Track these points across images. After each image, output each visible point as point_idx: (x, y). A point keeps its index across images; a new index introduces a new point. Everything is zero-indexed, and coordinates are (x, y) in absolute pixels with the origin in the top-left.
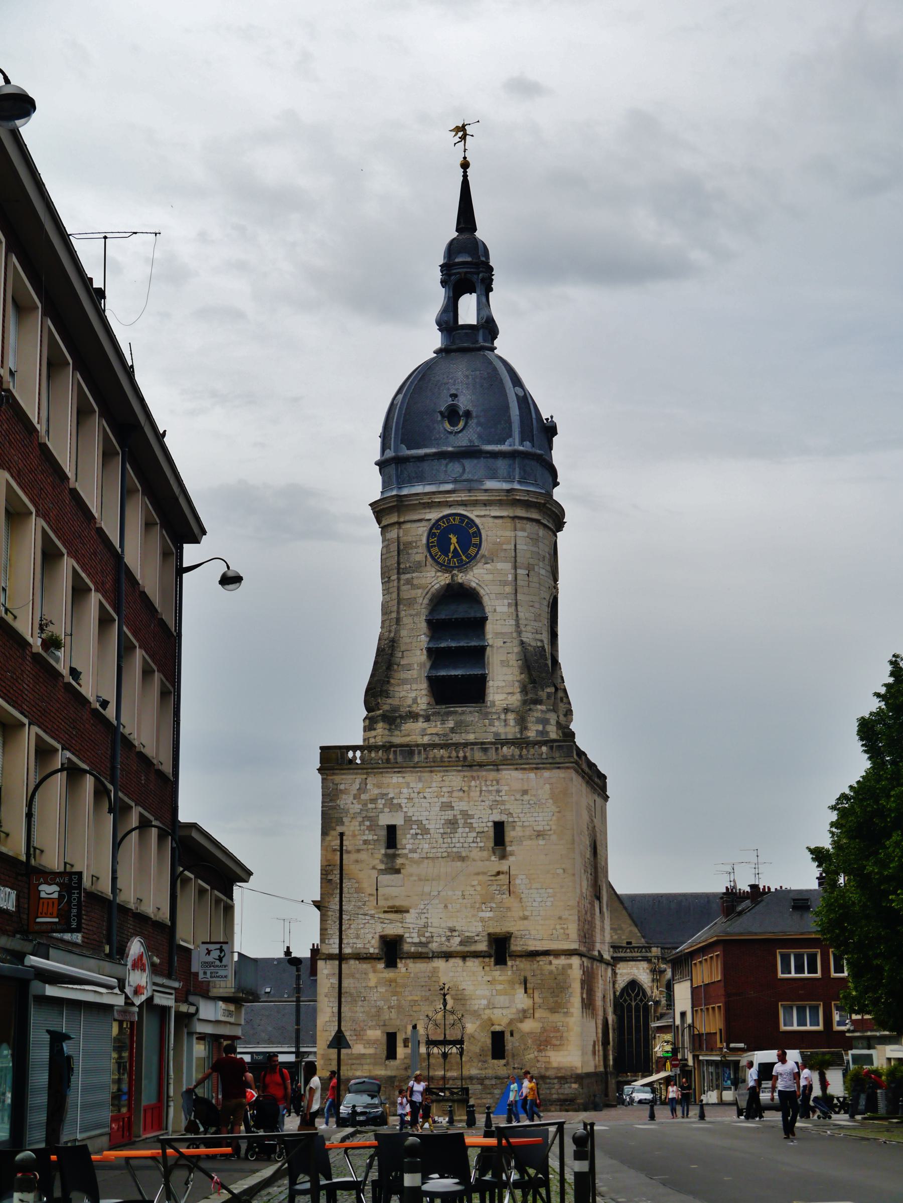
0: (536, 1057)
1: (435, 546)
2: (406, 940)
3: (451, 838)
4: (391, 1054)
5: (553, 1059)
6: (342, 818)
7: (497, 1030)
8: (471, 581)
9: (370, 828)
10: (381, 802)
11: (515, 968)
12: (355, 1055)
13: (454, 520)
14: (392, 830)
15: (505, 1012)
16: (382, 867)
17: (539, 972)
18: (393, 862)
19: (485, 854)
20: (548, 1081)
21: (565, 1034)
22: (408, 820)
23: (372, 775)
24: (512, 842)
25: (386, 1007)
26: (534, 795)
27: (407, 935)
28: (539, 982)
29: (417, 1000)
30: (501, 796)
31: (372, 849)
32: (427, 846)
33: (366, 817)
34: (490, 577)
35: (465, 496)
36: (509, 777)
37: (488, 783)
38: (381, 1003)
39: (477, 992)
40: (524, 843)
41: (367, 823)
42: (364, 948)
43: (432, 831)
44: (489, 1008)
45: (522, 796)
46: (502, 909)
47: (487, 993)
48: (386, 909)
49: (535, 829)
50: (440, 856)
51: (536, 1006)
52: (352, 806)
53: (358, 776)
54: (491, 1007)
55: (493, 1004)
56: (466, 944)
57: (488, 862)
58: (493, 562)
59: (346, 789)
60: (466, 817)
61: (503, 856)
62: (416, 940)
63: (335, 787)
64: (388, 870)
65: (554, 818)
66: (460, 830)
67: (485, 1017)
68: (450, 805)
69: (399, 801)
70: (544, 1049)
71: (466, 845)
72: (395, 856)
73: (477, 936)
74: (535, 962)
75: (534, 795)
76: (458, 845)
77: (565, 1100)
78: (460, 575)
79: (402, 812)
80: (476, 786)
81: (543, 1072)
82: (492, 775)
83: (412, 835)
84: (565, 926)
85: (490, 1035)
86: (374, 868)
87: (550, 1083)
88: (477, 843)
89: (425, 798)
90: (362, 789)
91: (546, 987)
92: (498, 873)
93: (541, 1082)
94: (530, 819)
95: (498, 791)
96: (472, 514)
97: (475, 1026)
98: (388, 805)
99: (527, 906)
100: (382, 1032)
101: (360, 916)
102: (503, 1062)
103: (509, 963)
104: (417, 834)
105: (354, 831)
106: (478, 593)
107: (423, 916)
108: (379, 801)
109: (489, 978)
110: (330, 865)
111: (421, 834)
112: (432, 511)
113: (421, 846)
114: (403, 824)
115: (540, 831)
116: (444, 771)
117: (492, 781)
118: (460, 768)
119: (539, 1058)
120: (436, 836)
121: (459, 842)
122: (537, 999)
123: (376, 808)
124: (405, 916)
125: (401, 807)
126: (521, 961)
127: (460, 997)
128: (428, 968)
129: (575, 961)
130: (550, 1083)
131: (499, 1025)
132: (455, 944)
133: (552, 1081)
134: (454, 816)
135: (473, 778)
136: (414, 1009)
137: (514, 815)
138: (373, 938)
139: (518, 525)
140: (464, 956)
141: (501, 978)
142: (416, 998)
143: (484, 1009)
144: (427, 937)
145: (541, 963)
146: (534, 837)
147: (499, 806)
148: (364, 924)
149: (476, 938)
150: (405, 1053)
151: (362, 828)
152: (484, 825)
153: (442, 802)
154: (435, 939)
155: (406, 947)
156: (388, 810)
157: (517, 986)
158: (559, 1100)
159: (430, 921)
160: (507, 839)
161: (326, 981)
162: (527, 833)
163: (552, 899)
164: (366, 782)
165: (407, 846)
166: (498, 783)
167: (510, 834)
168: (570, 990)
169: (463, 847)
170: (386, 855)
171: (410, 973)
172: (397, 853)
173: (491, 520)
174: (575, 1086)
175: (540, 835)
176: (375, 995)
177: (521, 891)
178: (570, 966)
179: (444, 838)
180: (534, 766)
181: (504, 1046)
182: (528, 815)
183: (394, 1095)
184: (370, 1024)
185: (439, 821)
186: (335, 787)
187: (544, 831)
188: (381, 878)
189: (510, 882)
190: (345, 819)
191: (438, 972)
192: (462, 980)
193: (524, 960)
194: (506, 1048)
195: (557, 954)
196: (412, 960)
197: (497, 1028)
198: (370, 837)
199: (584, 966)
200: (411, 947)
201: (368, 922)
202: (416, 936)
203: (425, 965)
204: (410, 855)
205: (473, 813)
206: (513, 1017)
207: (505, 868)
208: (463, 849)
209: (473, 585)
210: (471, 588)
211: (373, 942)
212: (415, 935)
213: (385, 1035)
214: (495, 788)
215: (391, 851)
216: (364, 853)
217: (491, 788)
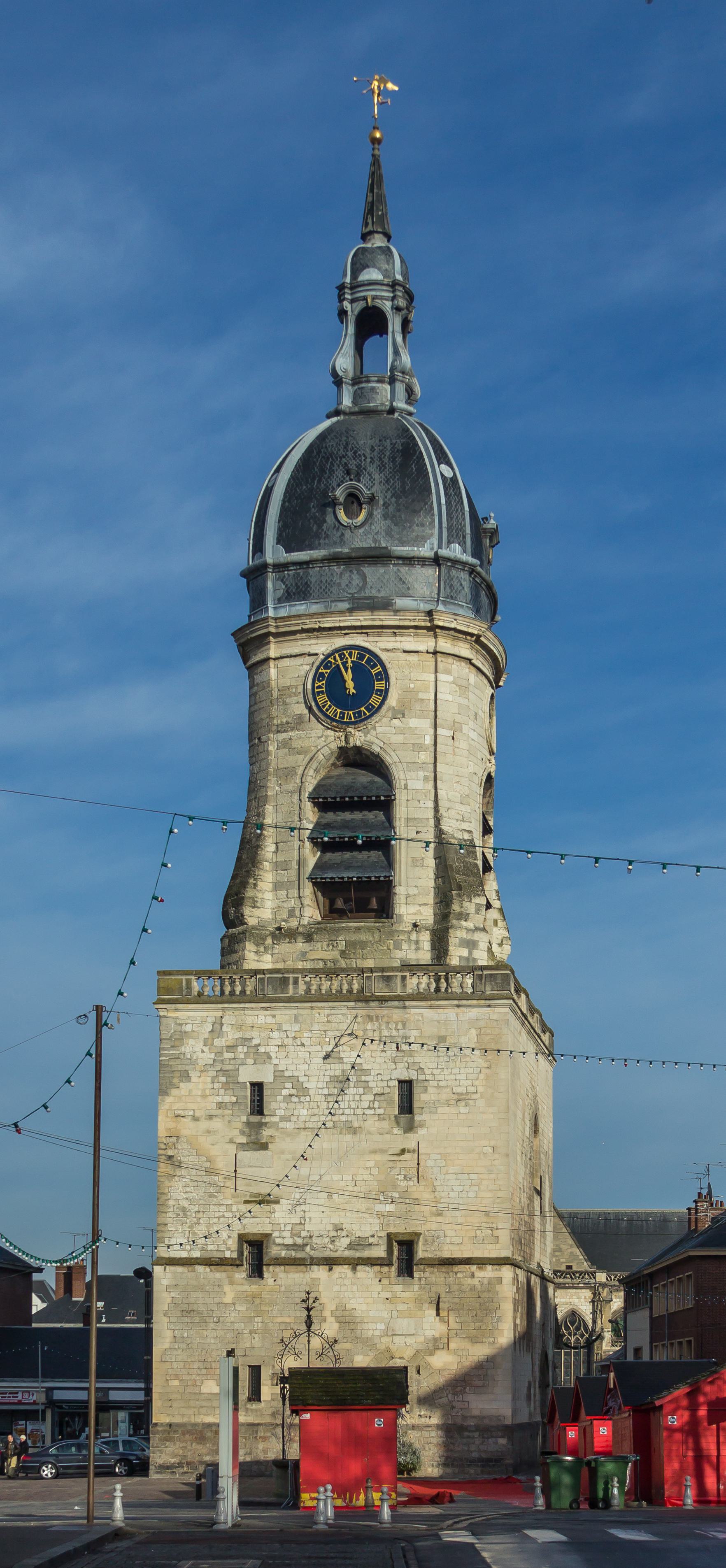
0: (450, 1402)
1: (322, 692)
2: (274, 1242)
5: (473, 1405)
6: (187, 1071)
7: (398, 1365)
8: (372, 743)
9: (226, 1086)
11: (423, 1282)
12: (207, 1395)
13: (350, 655)
14: (258, 1088)
15: (409, 1340)
16: (243, 1140)
17: (455, 1288)
18: (258, 1133)
19: (385, 1125)
20: (466, 1434)
21: (489, 1372)
22: (279, 1075)
23: (230, 1013)
24: (423, 1108)
27: (276, 1234)
28: (457, 1300)
31: (228, 1115)
34: (399, 739)
36: (420, 1019)
37: (390, 1026)
39: (371, 1314)
40: (440, 1110)
41: (223, 1079)
43: (312, 1092)
47: (385, 1314)
48: (248, 1198)
49: (454, 1091)
51: (452, 1334)
52: (201, 1055)
53: (211, 1013)
54: (390, 1334)
56: (356, 1247)
57: (388, 1135)
58: (404, 717)
59: (194, 1031)
60: (359, 1073)
61: (410, 1128)
62: (289, 1241)
63: (179, 1028)
64: (251, 1144)
65: (482, 1076)
66: (351, 1091)
67: (383, 1347)
70: (461, 1391)
72: (261, 1125)
73: (373, 1236)
74: (451, 1274)
76: (347, 1111)
77: (489, 1460)
79: (271, 1063)
80: (374, 1031)
81: (459, 1421)
82: (397, 1014)
83: (284, 1096)
84: (494, 1226)
86: (231, 1141)
87: (469, 1437)
89: (303, 1045)
91: (466, 1308)
92: (403, 1151)
93: (456, 1436)
94: (448, 1077)
98: (252, 1055)
99: (441, 1198)
103: (416, 1275)
104: (291, 1095)
105: (204, 1090)
106: (383, 761)
107: (298, 1209)
108: (240, 1049)
109: (389, 1295)
111: (297, 1096)
112: (320, 641)
113: (296, 1112)
115: (462, 1094)
117: (397, 1024)
118: (352, 1004)
119: (454, 1404)
120: (318, 1098)
121: (349, 1108)
122: (453, 1324)
123: (234, 1059)
124: (274, 1209)
125: (270, 1058)
126: (432, 1273)
127: (348, 1319)
128: (305, 1280)
129: (507, 1273)
130: (469, 1437)
131: (400, 1358)
133: (471, 1434)
134: (343, 1071)
135: (370, 1018)
137: (426, 1071)
138: (229, 1237)
139: (441, 666)
140: (354, 1263)
141: (404, 1295)
142: (288, 1320)
144: (303, 1238)
145: (459, 1275)
146: (453, 1102)
147: (405, 1059)
148: (219, 1218)
149: (371, 1240)
150: (272, 1394)
151: (216, 1085)
152: (385, 1084)
154: (314, 1240)
155: (274, 1251)
156: (253, 1062)
158: (481, 1460)
159: (307, 1215)
160: (416, 1105)
161: (165, 1295)
162: (444, 1097)
163: (476, 1188)
166: (404, 1025)
167: (420, 1098)
168: (499, 1313)
169: (354, 1114)
170: (248, 1124)
171: (280, 1286)
172: (263, 1121)
174: (503, 1441)
175: (461, 1099)
177: (434, 1177)
178: (500, 1280)
179: (328, 1102)
180: (456, 1002)
181: (407, 1387)
182: (446, 1071)
183: (257, 1448)
185: (322, 1078)
186: (179, 1028)
187: (467, 1093)
188: (242, 1155)
189: (418, 1164)
190: (191, 1074)
192: (351, 1296)
193: (436, 1270)
194: (410, 1389)
196: (282, 1267)
198: (227, 1099)
199: (518, 1281)
201: (224, 1216)
202: (289, 1235)
203: (301, 1275)
204: (281, 1125)
205: (369, 1067)
206: (420, 1347)
207: (413, 1145)
208: (354, 1118)
209: (376, 749)
210: (372, 753)
211: (230, 1242)
212: (288, 1234)
215: (255, 1119)
216: (219, 1120)
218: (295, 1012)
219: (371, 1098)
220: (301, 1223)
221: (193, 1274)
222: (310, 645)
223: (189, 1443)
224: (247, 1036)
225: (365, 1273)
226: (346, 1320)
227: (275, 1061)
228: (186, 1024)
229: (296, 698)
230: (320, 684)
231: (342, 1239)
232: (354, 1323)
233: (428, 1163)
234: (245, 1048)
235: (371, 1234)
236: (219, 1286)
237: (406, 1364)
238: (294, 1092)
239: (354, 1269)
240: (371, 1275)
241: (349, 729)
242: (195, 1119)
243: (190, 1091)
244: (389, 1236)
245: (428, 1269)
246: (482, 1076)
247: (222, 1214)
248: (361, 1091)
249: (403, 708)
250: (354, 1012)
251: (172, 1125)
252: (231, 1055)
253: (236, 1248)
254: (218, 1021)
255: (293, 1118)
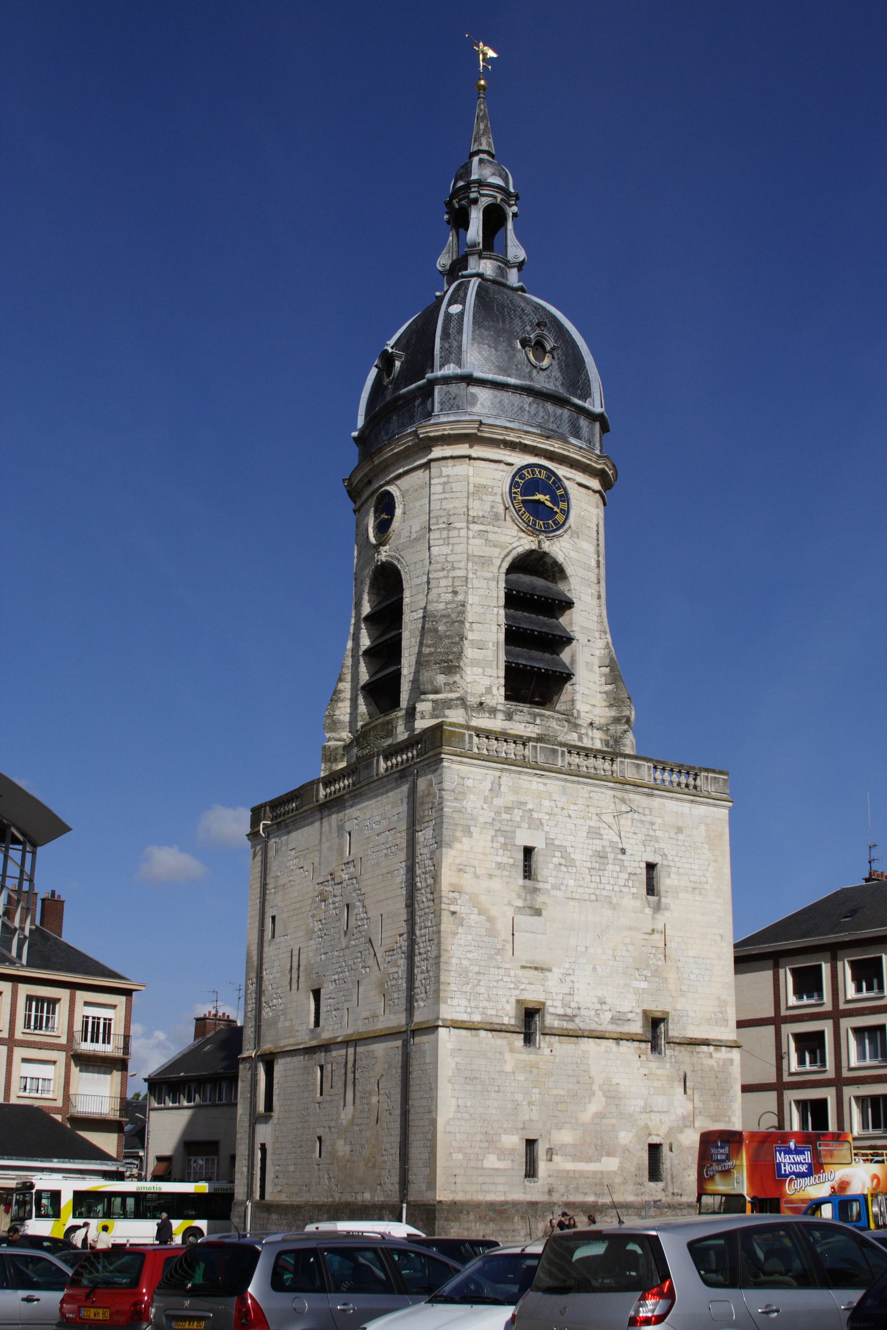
3: (600, 876)
4: (531, 1172)
9: (504, 846)
10: (517, 814)
11: (673, 1060)
13: (540, 472)
14: (528, 852)
15: (663, 1116)
16: (520, 903)
22: (550, 843)
23: (507, 774)
25: (525, 1103)
26: (690, 836)
27: (549, 1003)
29: (564, 1096)
30: (654, 830)
31: (506, 876)
32: (572, 882)
33: (499, 830)
35: (559, 448)
38: (519, 1097)
40: (681, 895)
41: (502, 840)
42: (497, 1016)
43: (578, 864)
44: (646, 1112)
45: (676, 834)
46: (657, 979)
48: (524, 964)
50: (587, 898)
51: (697, 1112)
53: (490, 772)
54: (648, 1111)
55: (650, 1107)
56: (618, 1022)
59: (475, 787)
61: (658, 908)
62: (560, 1011)
63: (461, 781)
64: (527, 909)
65: (711, 869)
66: (610, 867)
67: (641, 1123)
68: (597, 831)
69: (541, 816)
71: (617, 888)
72: (536, 890)
73: (631, 1012)
75: (690, 836)
76: (608, 887)
78: (548, 543)
83: (555, 865)
85: (647, 1148)
86: (509, 904)
88: (629, 887)
89: (570, 816)
90: (496, 789)
94: (686, 866)
95: (653, 824)
96: (562, 471)
97: (631, 1135)
98: (527, 820)
99: (684, 979)
100: (521, 1139)
101: (492, 970)
102: (661, 1185)
104: (560, 864)
107: (569, 978)
108: (516, 811)
110: (453, 892)
111: (565, 866)
113: (565, 882)
114: (544, 848)
116: (593, 785)
122: (698, 1103)
124: (547, 976)
125: (542, 824)
126: (680, 1051)
129: (735, 1054)
131: (658, 1135)
132: (605, 1024)
134: (603, 847)
136: (560, 1107)
137: (670, 858)
138: (508, 1002)
140: (618, 1040)
141: (659, 1072)
142: (562, 1092)
143: (641, 1113)
144: (573, 1008)
145: (701, 1055)
146: (690, 889)
147: (652, 843)
148: (497, 981)
149: (630, 1016)
152: (636, 864)
153: (589, 826)
155: (551, 1021)
157: (676, 1084)
159: (576, 986)
164: (500, 782)
165: (549, 878)
167: (665, 882)
168: (732, 1093)
170: (524, 887)
171: (555, 1056)
172: (537, 886)
173: (576, 486)
176: (513, 1084)
179: (591, 876)
180: (691, 798)
184: (505, 1126)
186: (461, 781)
187: (700, 883)
188: (519, 918)
190: (472, 829)
191: (588, 1058)
192: (615, 1071)
193: (683, 1049)
195: (718, 1045)
197: (655, 1140)
198: (505, 860)
200: (554, 1020)
203: (573, 1046)
204: (553, 892)
208: (613, 894)
212: (558, 1004)
213: (525, 1142)
214: (649, 818)
217: (643, 818)
218: (563, 783)
219: (626, 876)
220: (570, 994)
221: (476, 1039)
222: (504, 455)
223: (473, 1224)
224: (522, 800)
225: (627, 1047)
226: (613, 1096)
227: (546, 829)
228: (468, 778)
229: (492, 497)
230: (516, 490)
231: (606, 1013)
232: (619, 1098)
233: (671, 945)
234: (521, 811)
235: (629, 1009)
236: (500, 1053)
237: (662, 1141)
238: (563, 861)
239: (618, 1044)
240: (632, 1051)
241: (541, 537)
242: (477, 876)
243: (472, 847)
244: (645, 1012)
245: (677, 1048)
246: (711, 869)
247: (500, 977)
248: (618, 868)
249: (577, 530)
250: (612, 793)
251: (455, 880)
252: (508, 817)
253: (514, 1015)
254: (497, 782)
255: (563, 888)
